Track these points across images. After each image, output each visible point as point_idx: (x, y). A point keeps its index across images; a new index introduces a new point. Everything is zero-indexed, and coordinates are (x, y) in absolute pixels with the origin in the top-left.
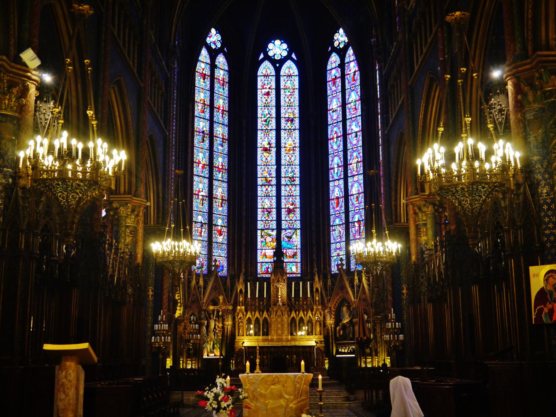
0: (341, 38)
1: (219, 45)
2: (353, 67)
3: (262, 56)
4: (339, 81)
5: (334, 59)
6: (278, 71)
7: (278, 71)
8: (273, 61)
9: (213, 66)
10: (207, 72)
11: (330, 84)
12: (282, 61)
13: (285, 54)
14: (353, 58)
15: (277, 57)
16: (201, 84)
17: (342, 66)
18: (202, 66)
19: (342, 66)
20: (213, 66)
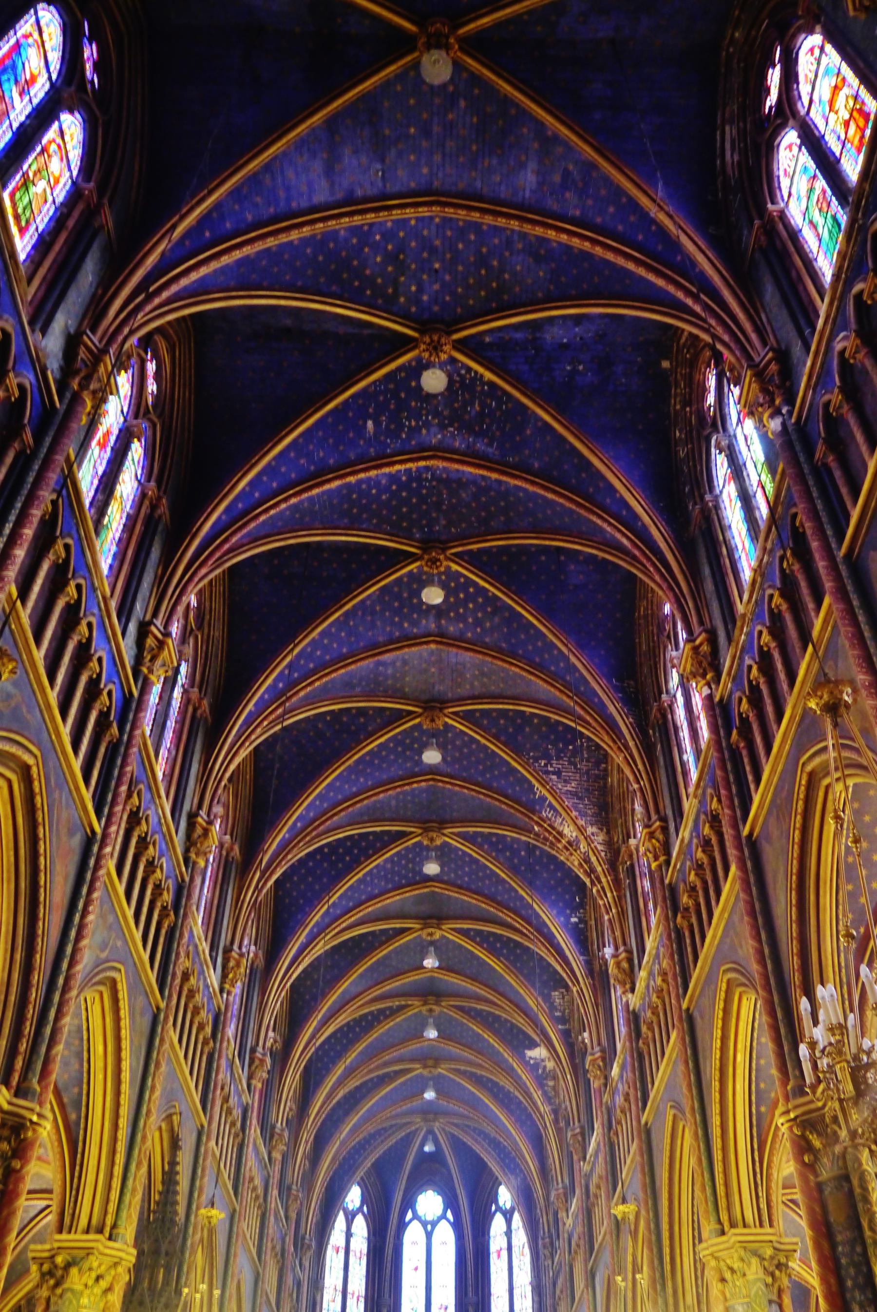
0: (505, 1196)
1: (358, 1204)
2: (520, 1238)
3: (409, 1215)
4: (505, 1254)
5: (498, 1224)
6: (429, 1235)
7: (429, 1235)
8: (424, 1224)
9: (349, 1235)
10: (342, 1244)
11: (493, 1257)
12: (434, 1224)
13: (439, 1212)
14: (521, 1224)
15: (429, 1218)
16: (333, 1261)
17: (509, 1233)
18: (337, 1237)
19: (509, 1233)
20: (349, 1235)
